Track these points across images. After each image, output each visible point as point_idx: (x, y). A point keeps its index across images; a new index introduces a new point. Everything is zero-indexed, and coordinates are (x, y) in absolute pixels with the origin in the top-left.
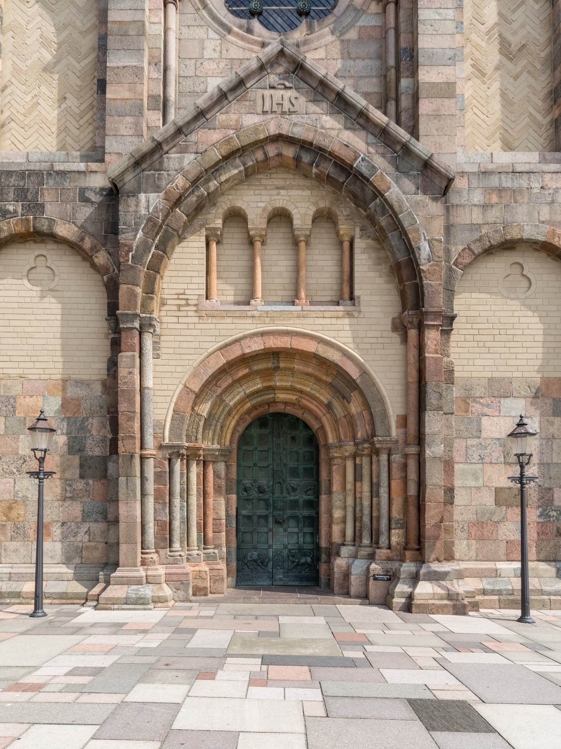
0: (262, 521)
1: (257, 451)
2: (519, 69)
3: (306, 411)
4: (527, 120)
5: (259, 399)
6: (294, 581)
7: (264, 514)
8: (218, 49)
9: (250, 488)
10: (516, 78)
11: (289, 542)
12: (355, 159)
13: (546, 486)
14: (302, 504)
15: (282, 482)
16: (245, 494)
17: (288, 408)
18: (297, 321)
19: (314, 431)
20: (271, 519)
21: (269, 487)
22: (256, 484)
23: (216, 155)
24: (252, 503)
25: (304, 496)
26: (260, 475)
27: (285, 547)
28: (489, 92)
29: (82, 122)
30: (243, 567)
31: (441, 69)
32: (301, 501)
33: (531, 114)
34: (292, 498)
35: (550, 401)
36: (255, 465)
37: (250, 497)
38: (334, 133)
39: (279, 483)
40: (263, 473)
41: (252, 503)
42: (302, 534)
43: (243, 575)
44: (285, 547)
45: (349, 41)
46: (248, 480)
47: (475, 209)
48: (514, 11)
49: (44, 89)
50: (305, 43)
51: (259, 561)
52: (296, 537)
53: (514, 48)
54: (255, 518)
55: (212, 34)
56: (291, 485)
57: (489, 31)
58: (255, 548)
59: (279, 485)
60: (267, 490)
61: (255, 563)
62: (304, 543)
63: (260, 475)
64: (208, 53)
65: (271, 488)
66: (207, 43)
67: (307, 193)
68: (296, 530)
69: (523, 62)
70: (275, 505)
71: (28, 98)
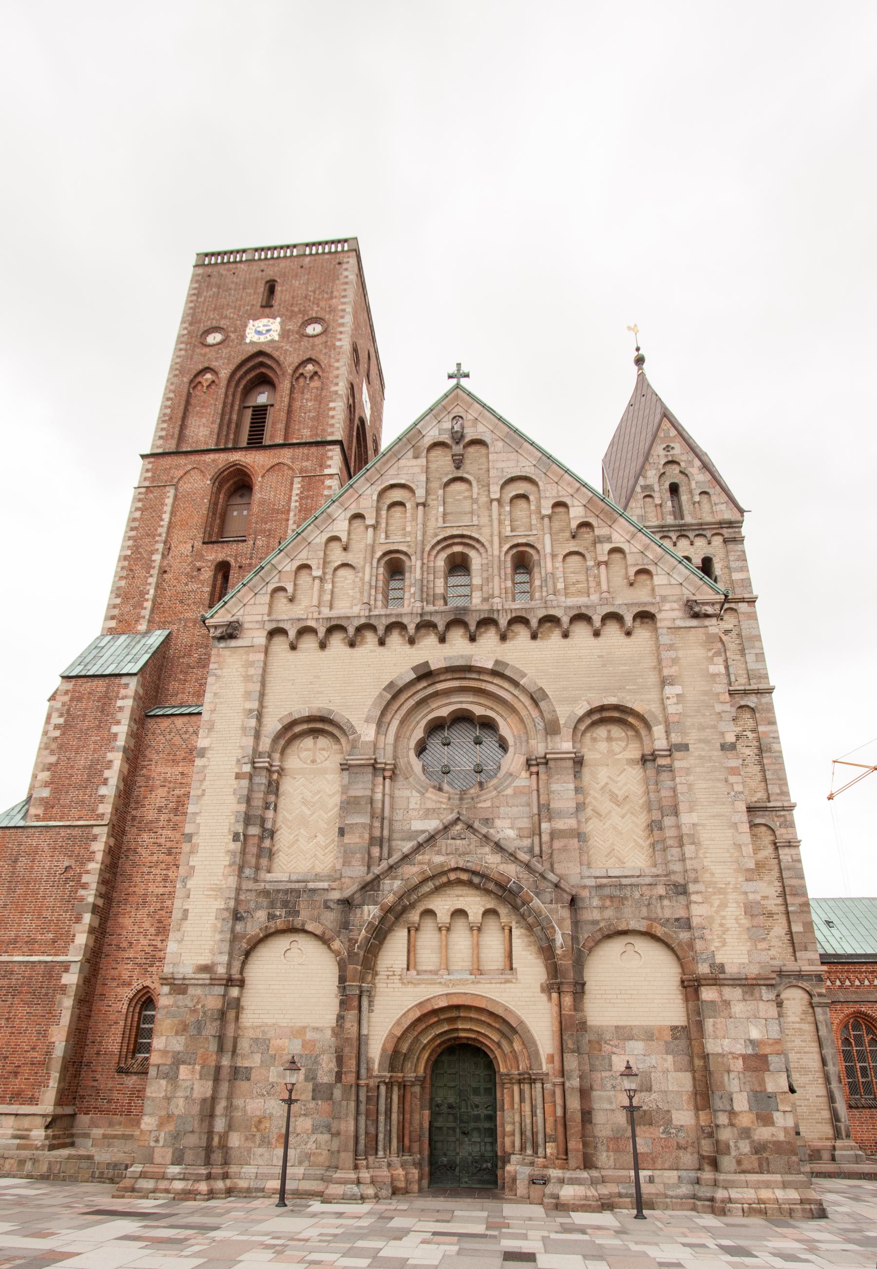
2: (624, 811)
4: (633, 844)
5: (446, 1037)
8: (419, 802)
10: (623, 817)
12: (509, 882)
13: (665, 1109)
18: (472, 986)
23: (416, 880)
28: (605, 827)
29: (326, 851)
31: (566, 820)
33: (635, 840)
35: (662, 1043)
38: (494, 866)
45: (507, 795)
47: (595, 910)
48: (619, 775)
49: (302, 831)
50: (478, 796)
53: (620, 798)
55: (415, 793)
57: (602, 788)
64: (412, 806)
66: (411, 799)
67: (478, 899)
69: (627, 807)
71: (292, 837)
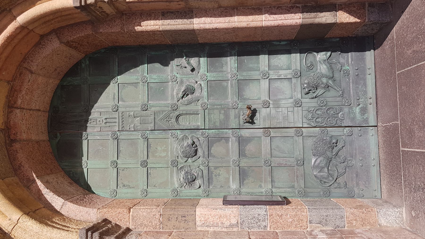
0: (250, 148)
1: (118, 162)
3: (25, 65)
6: (365, 85)
7: (237, 144)
9: (187, 173)
11: (290, 96)
14: (214, 74)
15: (177, 113)
16: (198, 182)
17: (19, 101)
19: (77, 56)
20: (245, 133)
21: (185, 138)
22: (180, 160)
24: (216, 168)
25: (201, 71)
26: (164, 154)
27: (298, 104)
30: (342, 184)
32: (211, 76)
34: (205, 94)
36: (144, 164)
37: (205, 172)
39: (178, 117)
40: (159, 148)
41: (216, 168)
42: (271, 72)
43: (358, 184)
44: (298, 104)
46: (172, 176)
51: (329, 154)
52: (278, 84)
54: (244, 163)
56: (180, 95)
58: (302, 162)
59: (180, 118)
60: (190, 142)
61: (334, 161)
62: (289, 68)
63: (164, 154)
65: (187, 133)
68: (265, 84)
70: (218, 124)
